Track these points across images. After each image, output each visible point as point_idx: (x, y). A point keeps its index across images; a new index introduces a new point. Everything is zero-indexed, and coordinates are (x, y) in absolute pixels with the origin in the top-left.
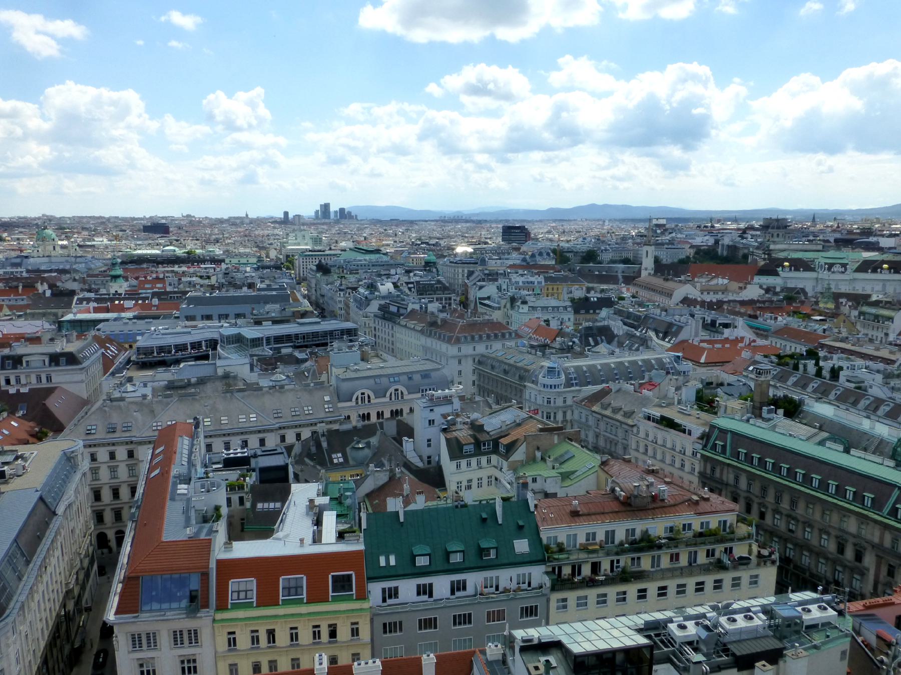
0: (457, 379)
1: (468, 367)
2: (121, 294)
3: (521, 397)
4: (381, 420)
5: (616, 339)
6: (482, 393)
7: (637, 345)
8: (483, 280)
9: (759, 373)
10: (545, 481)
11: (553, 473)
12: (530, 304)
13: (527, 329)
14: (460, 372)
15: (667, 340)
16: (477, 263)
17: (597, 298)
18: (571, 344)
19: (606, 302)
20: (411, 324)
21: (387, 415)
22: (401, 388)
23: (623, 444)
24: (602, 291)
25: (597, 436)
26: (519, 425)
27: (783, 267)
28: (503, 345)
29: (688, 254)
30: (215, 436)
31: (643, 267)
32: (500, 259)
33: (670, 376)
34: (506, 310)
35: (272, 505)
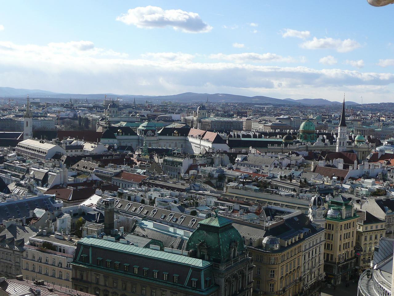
15: (44, 186)
27: (118, 132)
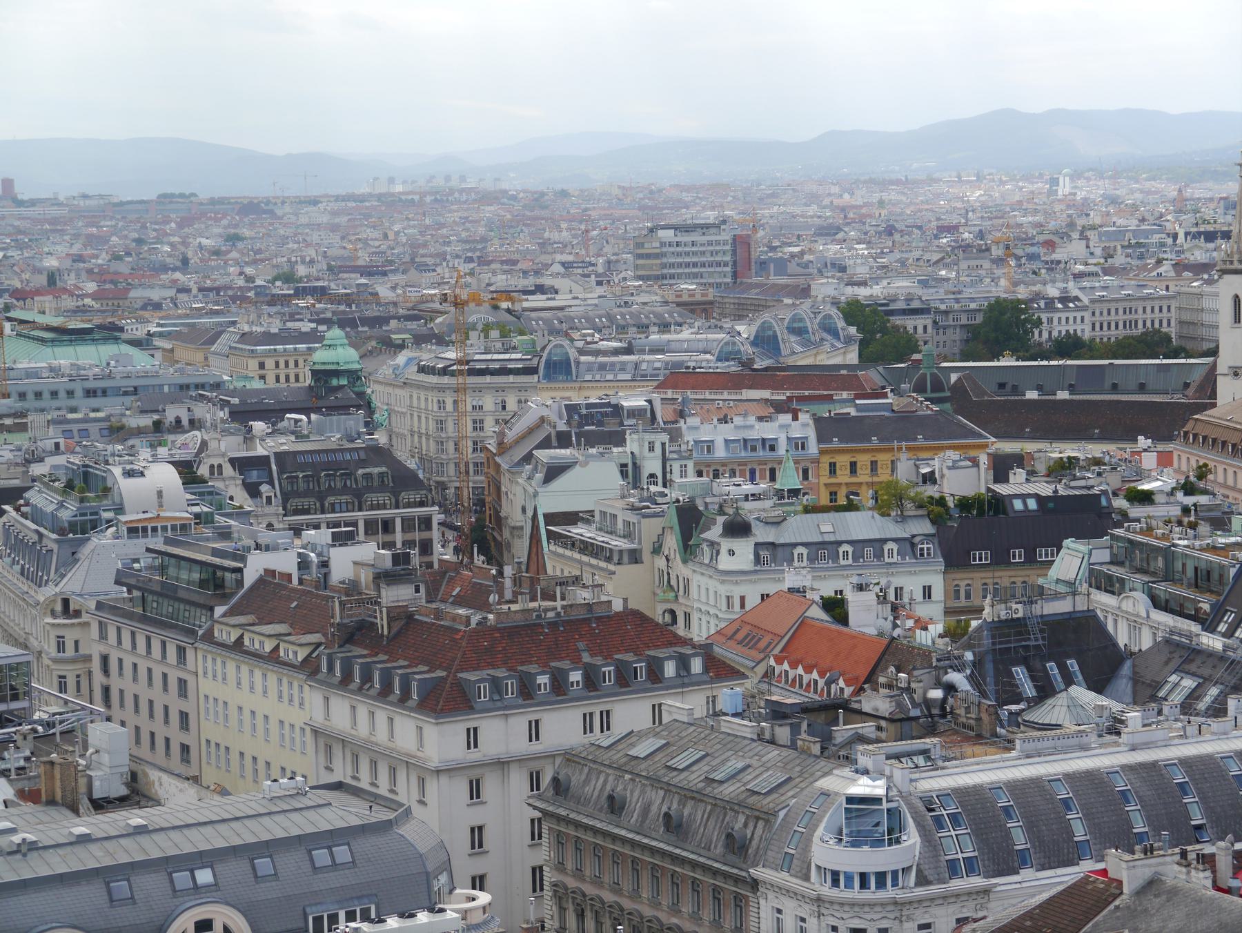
0: (465, 866)
5: (1126, 669)
7: (1214, 691)
8: (563, 440)
12: (762, 534)
14: (477, 832)
18: (937, 694)
20: (260, 639)
24: (1063, 468)
28: (657, 710)
32: (629, 351)
34: (661, 562)
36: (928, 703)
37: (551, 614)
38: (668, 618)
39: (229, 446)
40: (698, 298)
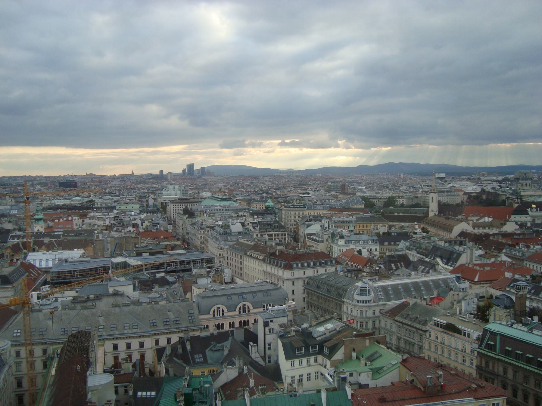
0: (291, 297)
1: (299, 287)
2: (42, 232)
3: (340, 310)
4: (232, 329)
5: (412, 264)
6: (310, 308)
7: (427, 269)
8: (310, 220)
9: (518, 288)
10: (360, 375)
11: (367, 369)
12: (346, 238)
13: (344, 258)
14: (293, 291)
15: (450, 264)
16: (305, 207)
17: (397, 233)
19: (405, 236)
21: (237, 325)
22: (248, 304)
23: (418, 345)
25: (399, 339)
26: (339, 332)
27: (532, 208)
28: (326, 270)
29: (462, 200)
30: (120, 338)
31: (430, 209)
33: (452, 292)
35: (149, 393)
36: (376, 270)
37: (307, 252)
38: (329, 253)
39: (250, 220)
40: (335, 195)
